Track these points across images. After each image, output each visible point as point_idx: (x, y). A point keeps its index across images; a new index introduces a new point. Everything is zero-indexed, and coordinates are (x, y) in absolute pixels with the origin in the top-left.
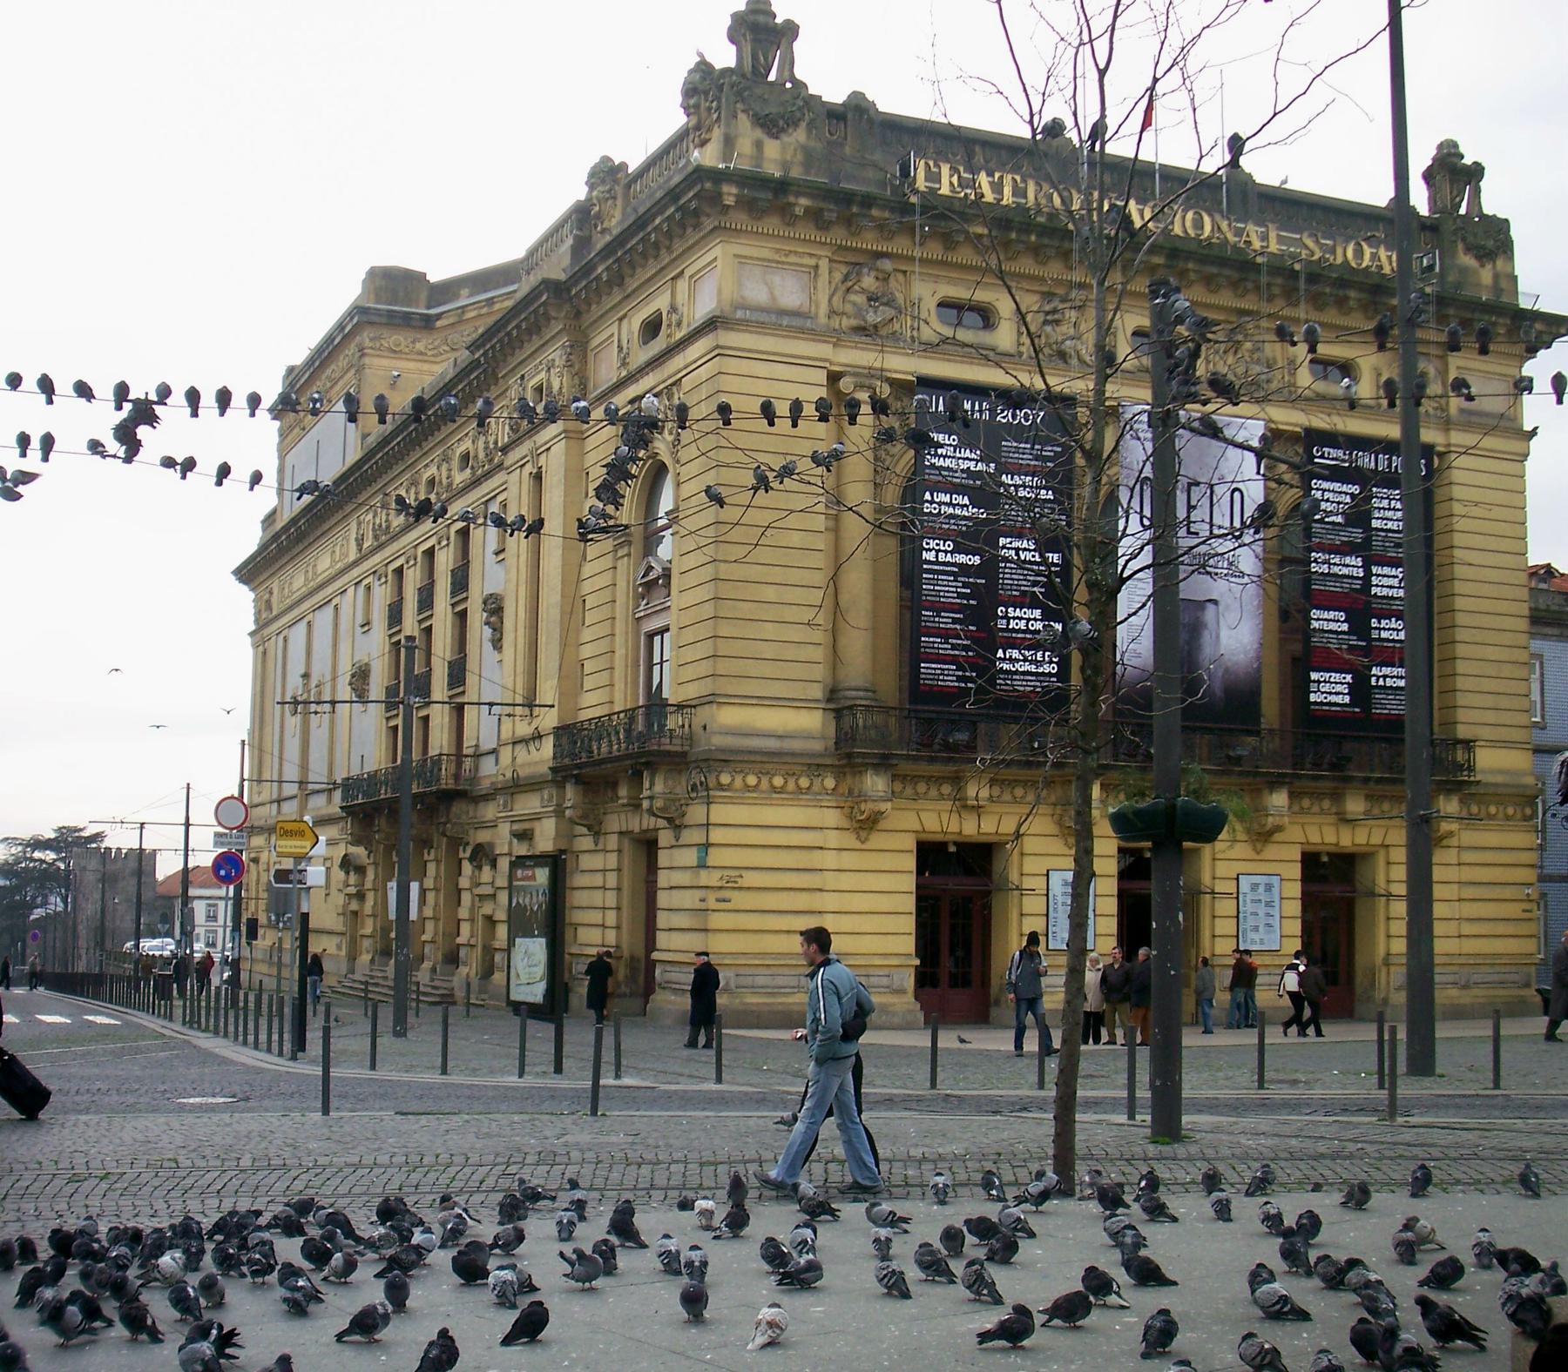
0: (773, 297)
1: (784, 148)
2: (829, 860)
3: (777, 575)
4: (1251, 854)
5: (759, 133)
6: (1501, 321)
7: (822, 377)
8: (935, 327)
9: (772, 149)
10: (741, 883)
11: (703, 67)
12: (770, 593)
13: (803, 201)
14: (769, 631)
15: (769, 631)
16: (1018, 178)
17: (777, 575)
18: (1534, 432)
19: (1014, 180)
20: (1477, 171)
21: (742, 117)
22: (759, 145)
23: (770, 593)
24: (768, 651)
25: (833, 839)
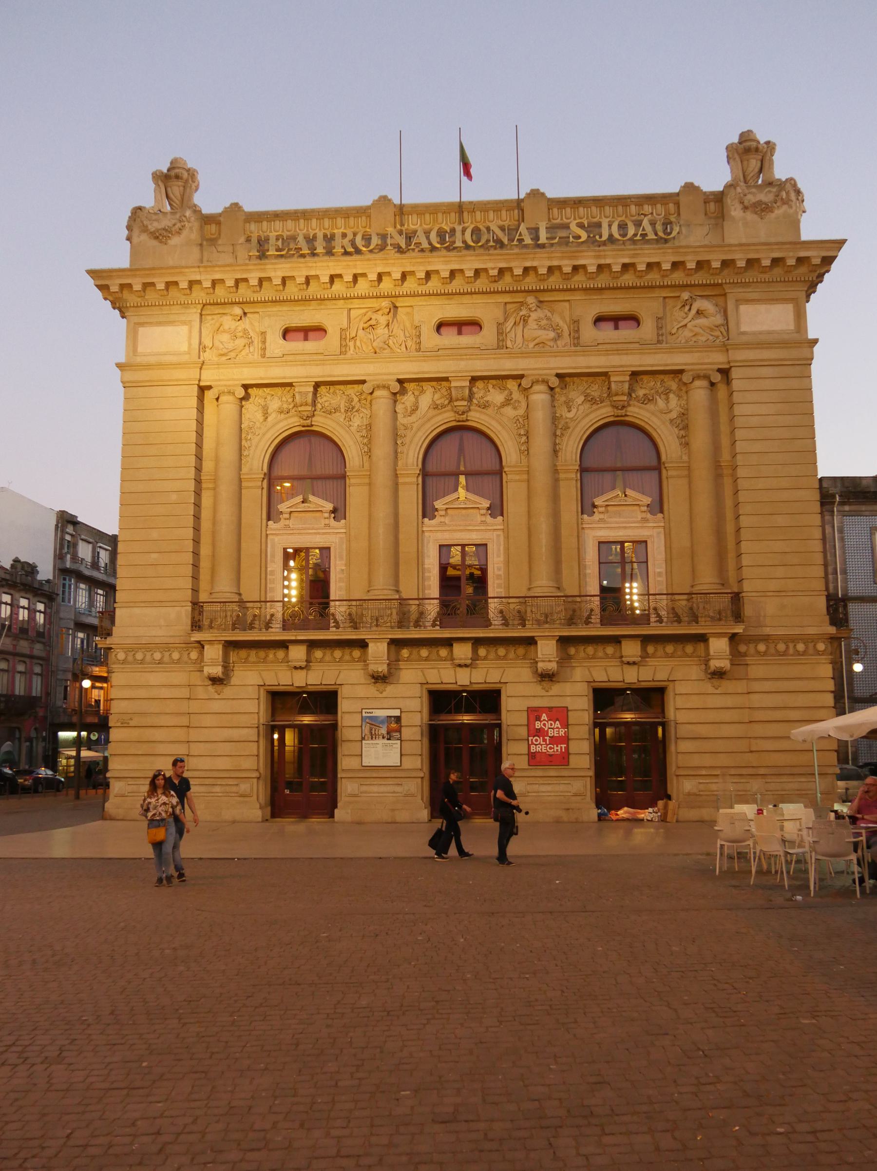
2: (194, 706)
4: (544, 693)
7: (196, 388)
8: (277, 345)
10: (132, 723)
11: (137, 211)
18: (816, 341)
20: (770, 146)
25: (201, 692)
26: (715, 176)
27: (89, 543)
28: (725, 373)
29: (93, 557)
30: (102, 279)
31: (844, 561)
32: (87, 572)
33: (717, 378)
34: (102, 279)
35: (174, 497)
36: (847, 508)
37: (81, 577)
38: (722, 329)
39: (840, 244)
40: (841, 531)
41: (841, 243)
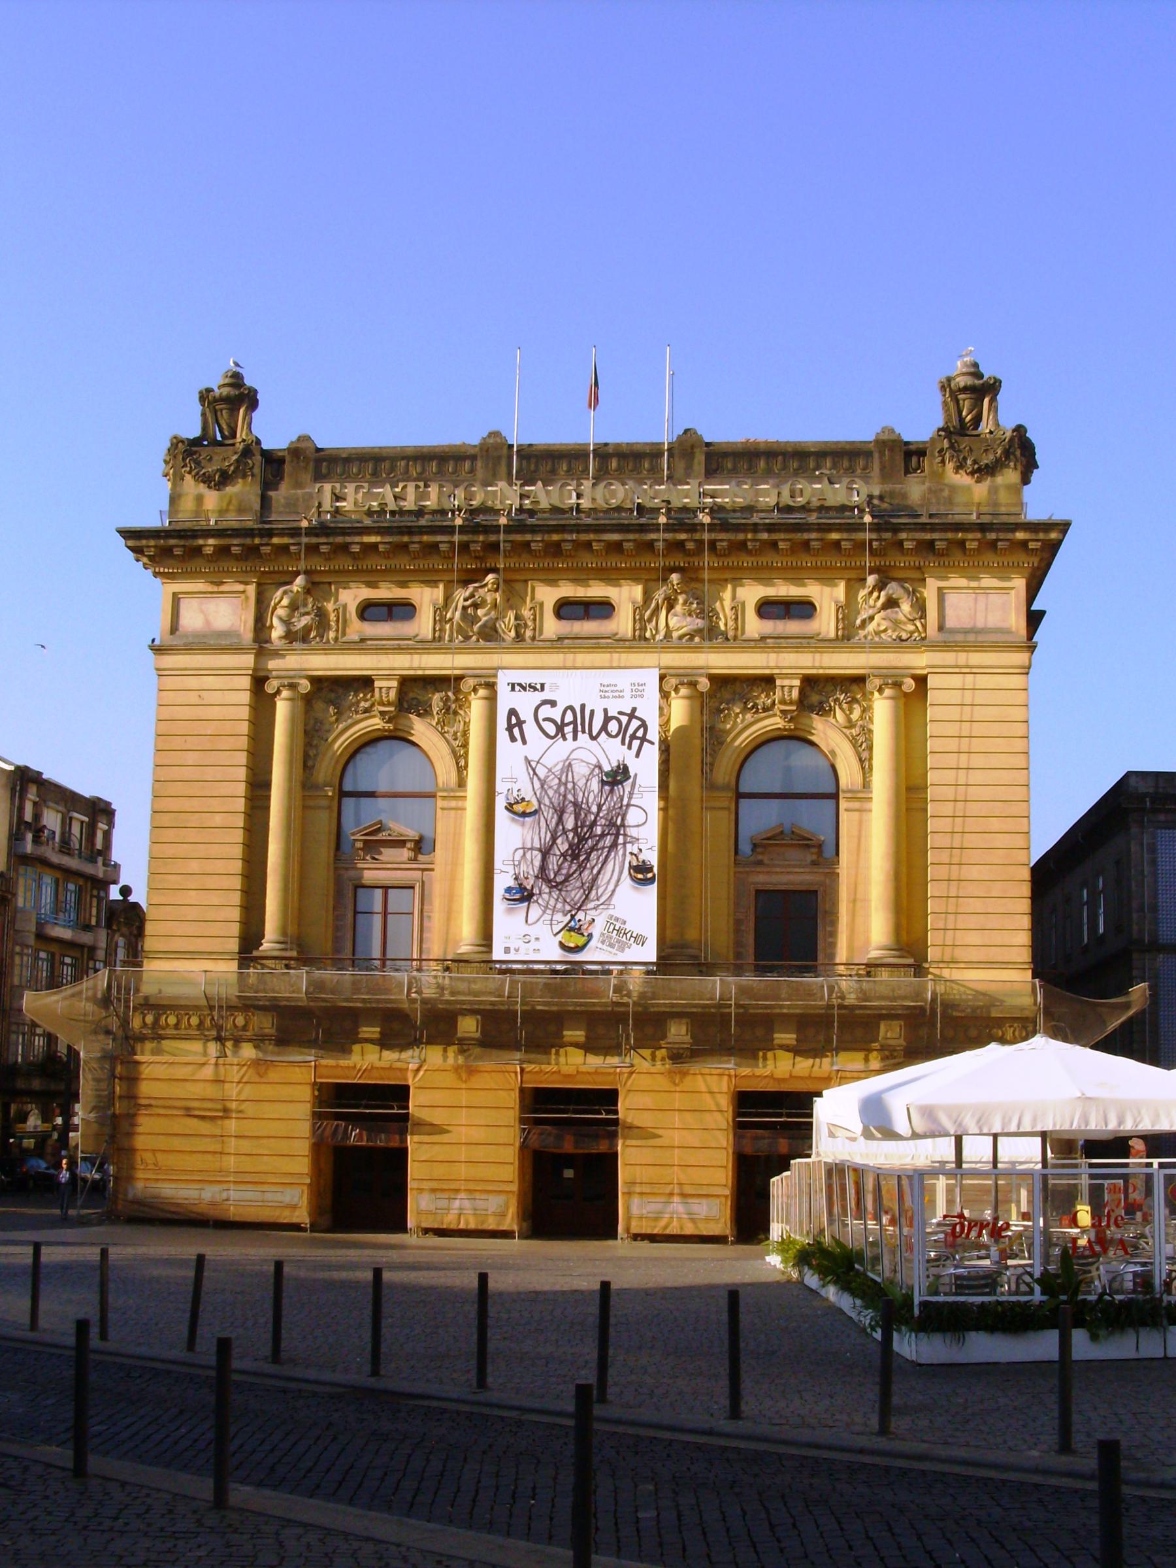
0: (207, 622)
1: (221, 498)
3: (202, 850)
5: (202, 488)
6: (970, 536)
9: (212, 499)
11: (176, 442)
12: (194, 866)
13: (211, 541)
14: (193, 897)
15: (193, 897)
16: (421, 484)
17: (202, 850)
19: (417, 487)
21: (188, 477)
22: (200, 499)
23: (194, 866)
24: (192, 913)
26: (922, 422)
27: (58, 811)
28: (921, 680)
29: (63, 834)
30: (134, 537)
31: (1155, 895)
32: (56, 858)
33: (909, 685)
34: (134, 537)
35: (218, 820)
36: (1162, 817)
37: (45, 863)
38: (918, 624)
39: (1064, 527)
40: (1153, 850)
41: (1064, 527)
